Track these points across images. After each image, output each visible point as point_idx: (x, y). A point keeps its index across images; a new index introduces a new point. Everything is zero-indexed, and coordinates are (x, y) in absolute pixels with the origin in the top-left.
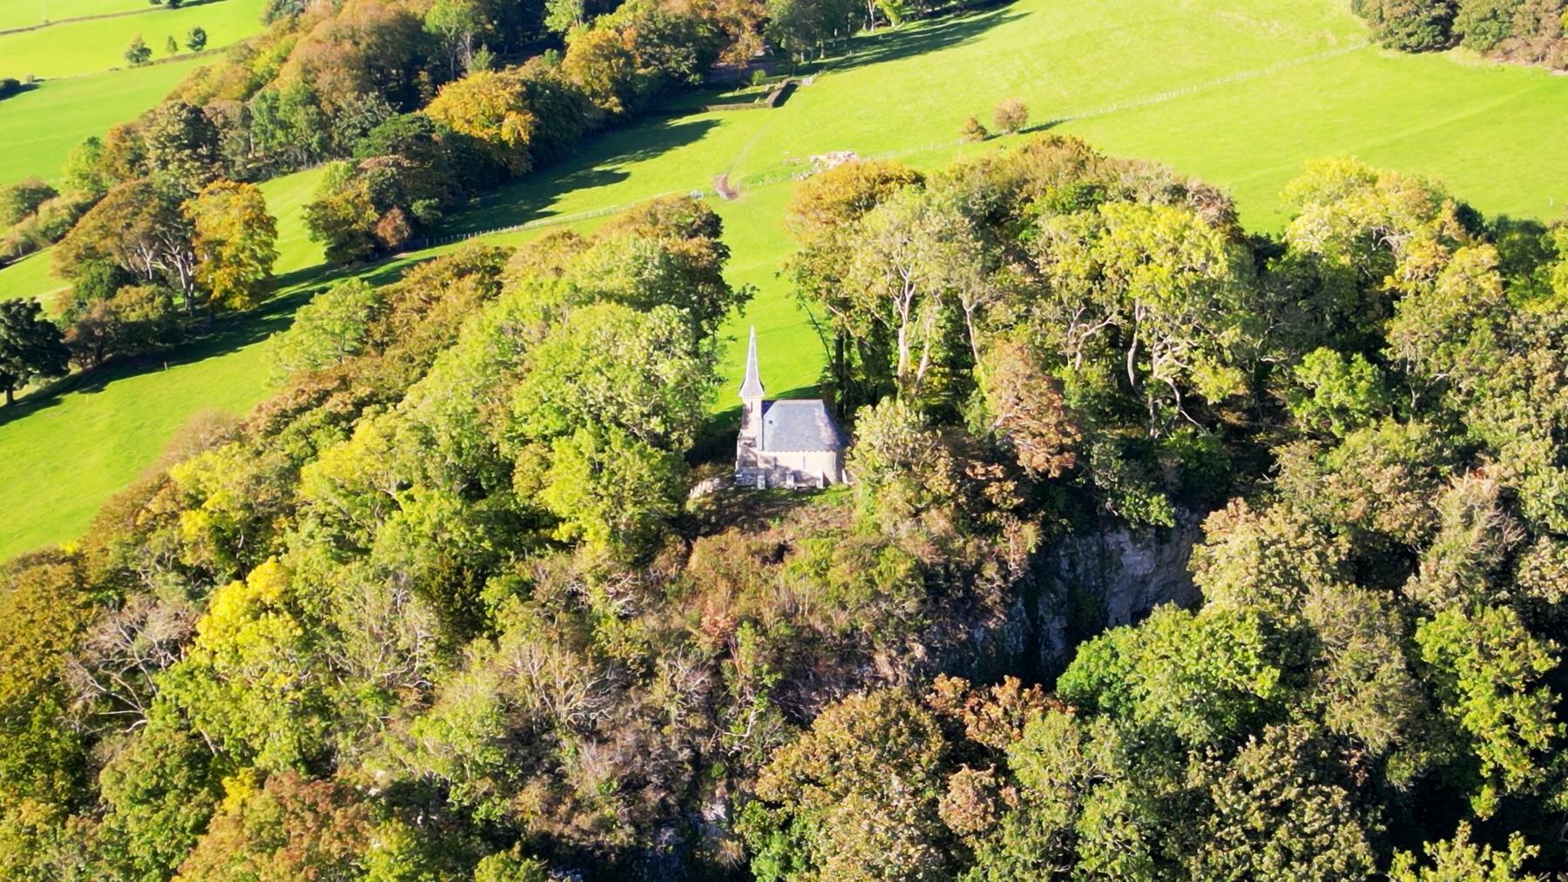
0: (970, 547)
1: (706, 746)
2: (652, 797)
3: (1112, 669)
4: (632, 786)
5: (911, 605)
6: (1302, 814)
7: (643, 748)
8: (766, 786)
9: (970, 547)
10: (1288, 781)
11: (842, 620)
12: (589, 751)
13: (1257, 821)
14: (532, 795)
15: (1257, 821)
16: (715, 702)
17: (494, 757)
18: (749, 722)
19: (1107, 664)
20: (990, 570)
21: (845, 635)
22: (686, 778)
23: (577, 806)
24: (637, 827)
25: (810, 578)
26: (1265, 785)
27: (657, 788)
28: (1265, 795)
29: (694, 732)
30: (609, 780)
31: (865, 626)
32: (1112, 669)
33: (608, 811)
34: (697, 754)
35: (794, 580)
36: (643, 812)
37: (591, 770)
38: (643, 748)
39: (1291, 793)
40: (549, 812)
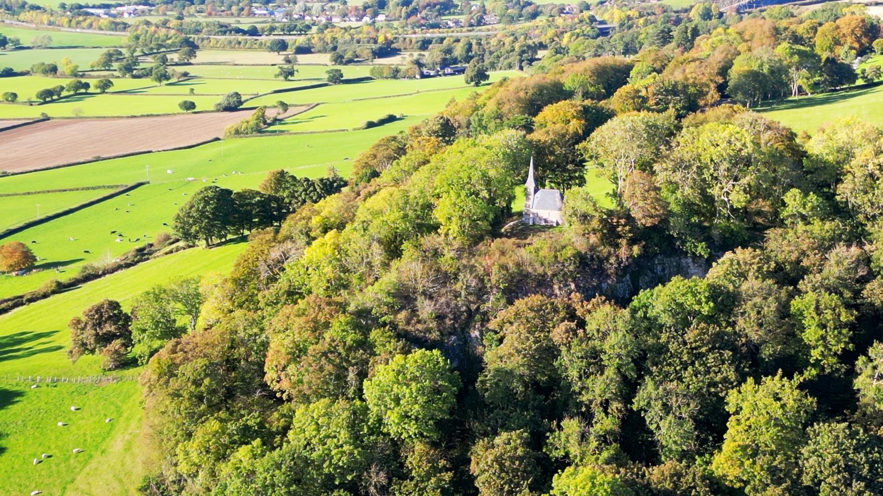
0: (605, 250)
1: (474, 307)
2: (448, 322)
3: (650, 300)
4: (440, 318)
5: (571, 268)
6: (707, 359)
7: (448, 305)
8: (493, 325)
9: (605, 250)
10: (704, 345)
11: (540, 270)
12: (427, 302)
13: (685, 358)
14: (402, 315)
15: (685, 358)
16: (481, 292)
17: (390, 300)
18: (492, 300)
19: (648, 298)
20: (612, 260)
21: (540, 275)
22: (463, 317)
23: (419, 322)
24: (441, 333)
25: (533, 253)
26: (693, 345)
27: (450, 320)
28: (692, 349)
29: (471, 302)
30: (432, 314)
31: (549, 273)
32: (650, 300)
33: (431, 325)
34: (470, 310)
35: (524, 254)
36: (444, 328)
37: (426, 309)
38: (448, 305)
39: (704, 350)
40: (408, 323)
